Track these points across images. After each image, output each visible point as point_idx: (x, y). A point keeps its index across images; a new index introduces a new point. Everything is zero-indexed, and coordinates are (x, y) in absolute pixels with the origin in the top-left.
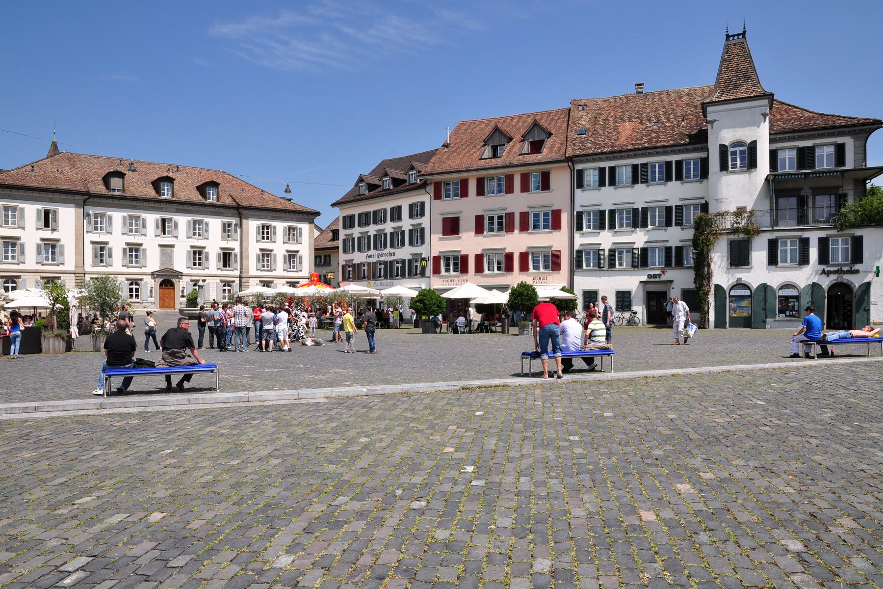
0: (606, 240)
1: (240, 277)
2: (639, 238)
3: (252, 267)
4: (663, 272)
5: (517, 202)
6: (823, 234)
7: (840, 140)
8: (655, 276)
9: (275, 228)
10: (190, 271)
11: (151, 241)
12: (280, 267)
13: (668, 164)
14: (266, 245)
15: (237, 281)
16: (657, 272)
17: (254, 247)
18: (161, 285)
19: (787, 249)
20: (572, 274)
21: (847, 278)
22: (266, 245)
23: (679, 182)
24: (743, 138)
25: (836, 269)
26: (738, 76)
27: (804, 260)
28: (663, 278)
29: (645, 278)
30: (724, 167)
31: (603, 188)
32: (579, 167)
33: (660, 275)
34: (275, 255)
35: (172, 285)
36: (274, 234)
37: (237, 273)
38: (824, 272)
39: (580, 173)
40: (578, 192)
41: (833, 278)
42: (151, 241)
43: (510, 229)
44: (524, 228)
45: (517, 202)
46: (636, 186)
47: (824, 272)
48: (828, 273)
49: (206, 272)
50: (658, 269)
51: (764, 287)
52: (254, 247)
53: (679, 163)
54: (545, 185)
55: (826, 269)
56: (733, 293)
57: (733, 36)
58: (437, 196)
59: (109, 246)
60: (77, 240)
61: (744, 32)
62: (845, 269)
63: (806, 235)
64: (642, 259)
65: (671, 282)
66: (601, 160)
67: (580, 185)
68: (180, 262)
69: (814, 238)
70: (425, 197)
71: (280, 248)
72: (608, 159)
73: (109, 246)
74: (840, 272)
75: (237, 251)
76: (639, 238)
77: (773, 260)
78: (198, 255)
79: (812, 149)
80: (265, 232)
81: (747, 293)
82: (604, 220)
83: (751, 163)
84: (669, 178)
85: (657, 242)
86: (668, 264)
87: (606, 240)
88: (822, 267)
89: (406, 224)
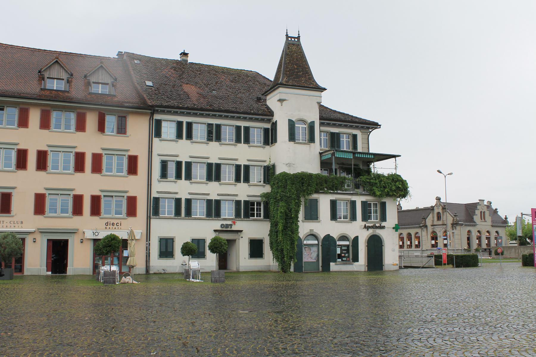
0: (183, 189)
2: (214, 190)
4: (234, 223)
5: (90, 142)
6: (364, 198)
7: (355, 132)
8: (227, 226)
13: (238, 128)
16: (229, 222)
19: (343, 210)
20: (149, 219)
21: (379, 232)
23: (246, 145)
24: (305, 118)
25: (372, 225)
26: (295, 69)
27: (353, 218)
28: (234, 228)
29: (219, 228)
30: (292, 137)
31: (180, 141)
32: (157, 117)
33: (231, 225)
38: (365, 227)
39: (159, 123)
40: (156, 140)
41: (371, 231)
44: (97, 168)
45: (90, 142)
46: (211, 143)
47: (365, 227)
48: (367, 228)
50: (229, 219)
51: (328, 238)
53: (247, 129)
54: (122, 130)
55: (367, 225)
56: (305, 242)
57: (291, 37)
61: (298, 38)
62: (377, 225)
63: (354, 198)
64: (214, 209)
65: (242, 231)
66: (182, 114)
67: (158, 134)
69: (359, 200)
72: (189, 114)
74: (374, 227)
76: (214, 190)
77: (334, 216)
79: (338, 134)
81: (316, 242)
82: (184, 170)
83: (312, 139)
84: (238, 140)
85: (228, 195)
86: (238, 215)
87: (183, 189)
88: (364, 223)
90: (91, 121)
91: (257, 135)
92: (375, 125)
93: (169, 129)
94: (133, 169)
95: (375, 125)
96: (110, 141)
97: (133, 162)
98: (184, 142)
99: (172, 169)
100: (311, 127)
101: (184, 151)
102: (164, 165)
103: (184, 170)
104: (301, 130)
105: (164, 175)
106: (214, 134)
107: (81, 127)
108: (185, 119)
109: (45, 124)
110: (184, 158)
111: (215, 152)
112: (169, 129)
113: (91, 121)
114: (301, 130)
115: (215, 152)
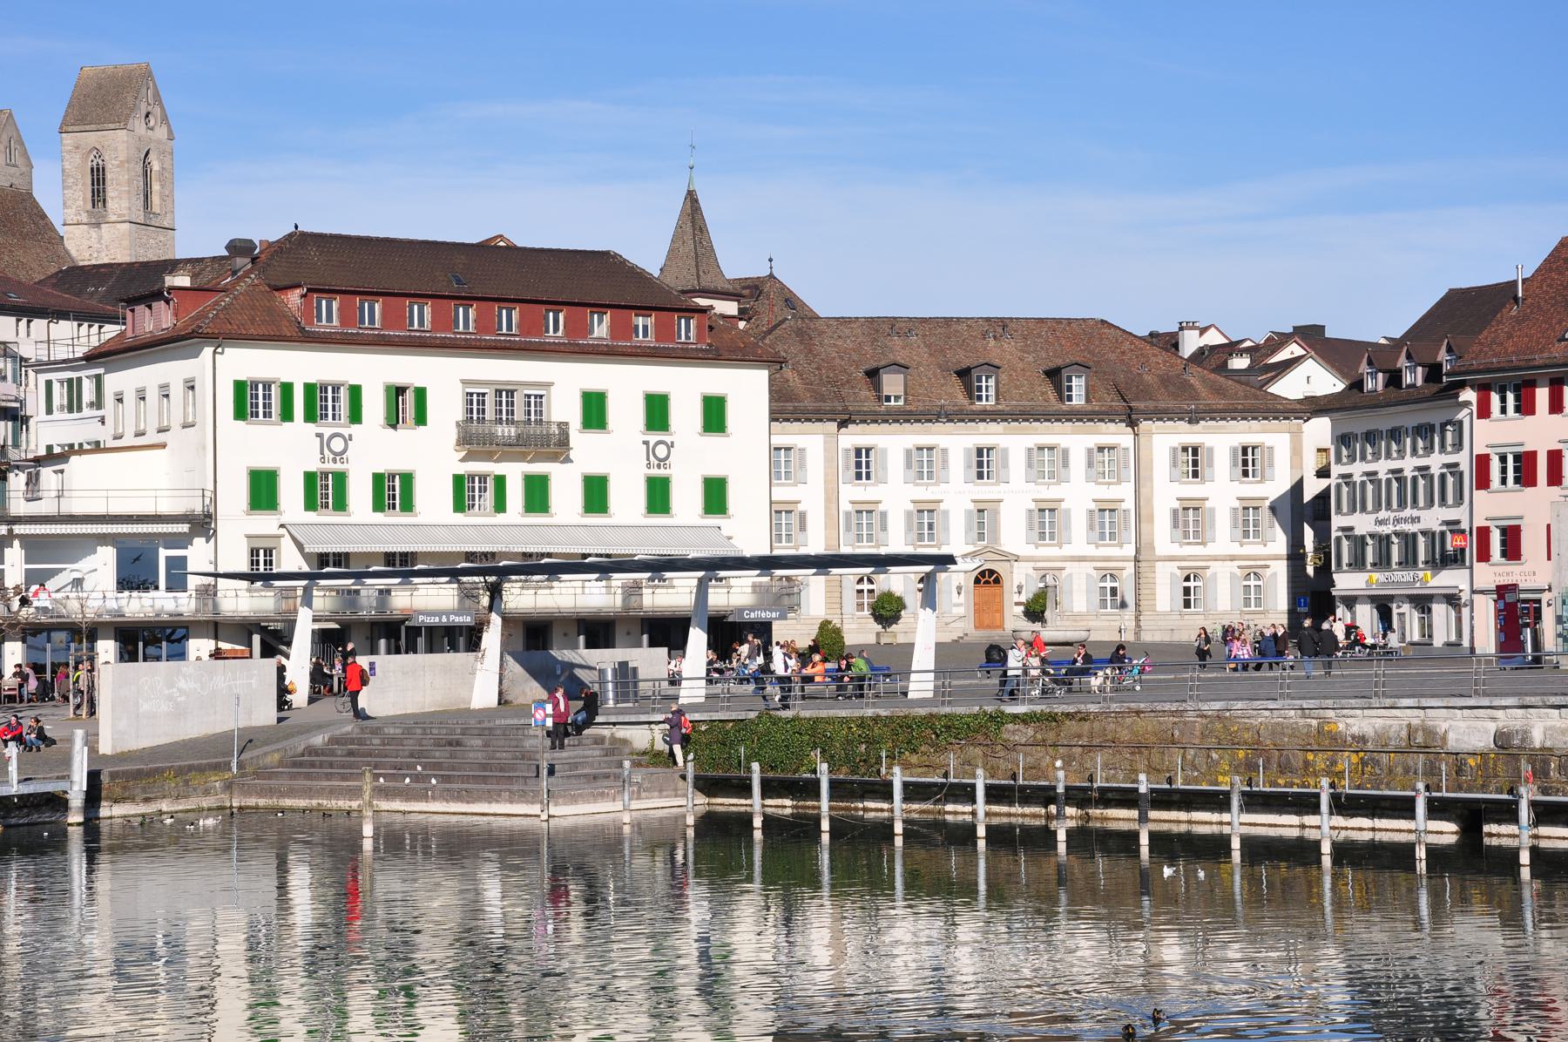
1: (1137, 560)
3: (1163, 538)
9: (1211, 450)
10: (1030, 551)
11: (957, 494)
12: (1223, 539)
14: (1193, 490)
15: (1130, 567)
17: (1167, 492)
18: (977, 581)
22: (1193, 490)
34: (1212, 510)
35: (997, 581)
36: (1211, 465)
37: (1130, 550)
42: (957, 494)
49: (1067, 551)
52: (1167, 492)
59: (881, 507)
60: (828, 500)
68: (1013, 535)
71: (1222, 491)
73: (881, 507)
75: (1129, 504)
78: (1046, 519)
80: (1194, 461)
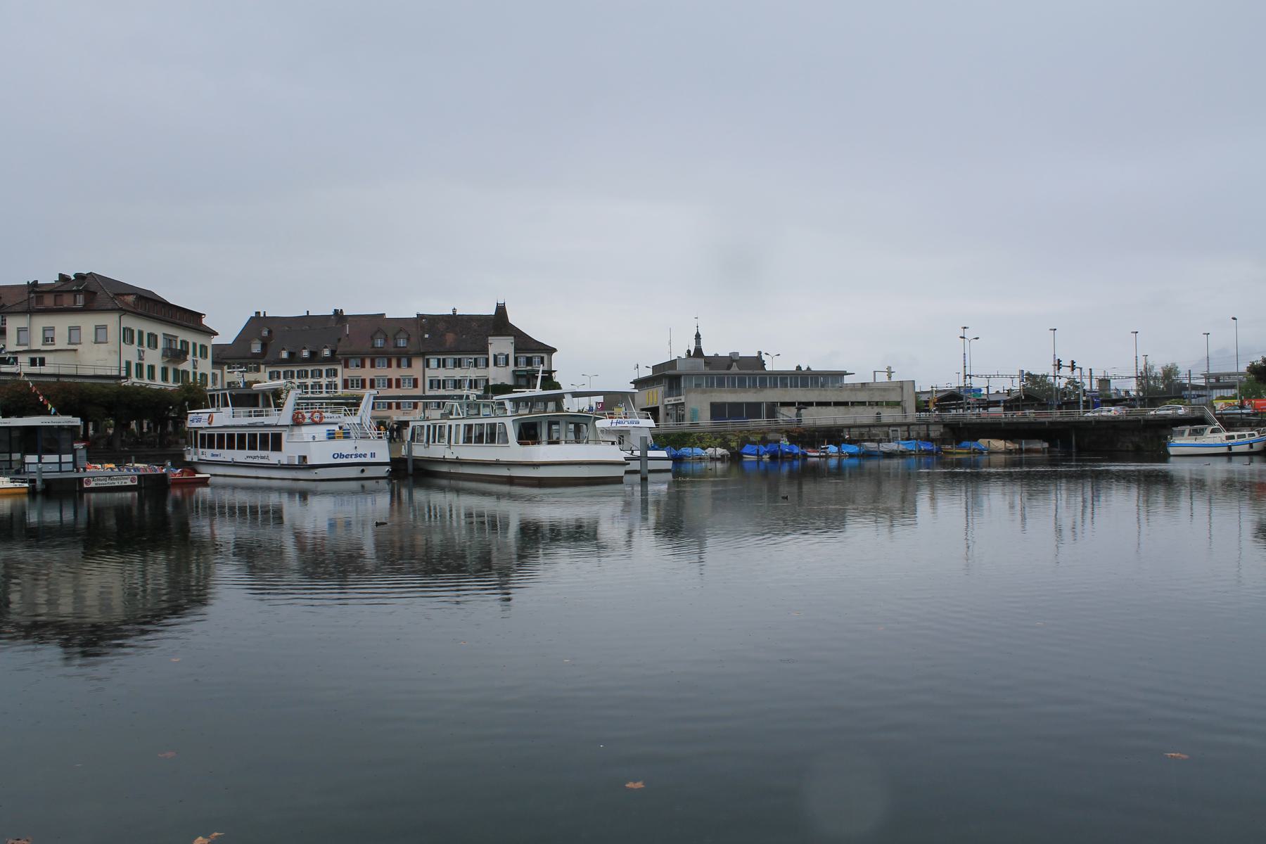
30: (496, 364)
39: (428, 361)
43: (390, 386)
44: (398, 386)
45: (394, 373)
54: (409, 365)
58: (346, 366)
67: (428, 366)
70: (339, 368)
83: (507, 364)
89: (324, 381)
90: (394, 362)
91: (482, 362)
92: (555, 350)
93: (433, 363)
94: (415, 385)
95: (555, 350)
96: (404, 372)
97: (416, 381)
98: (441, 369)
99: (435, 384)
100: (507, 357)
101: (442, 374)
102: (431, 382)
103: (441, 384)
104: (501, 359)
105: (431, 387)
106: (458, 364)
107: (389, 366)
108: (441, 357)
109: (373, 366)
110: (441, 378)
111: (458, 373)
112: (433, 363)
113: (394, 362)
114: (501, 359)
115: (458, 373)
